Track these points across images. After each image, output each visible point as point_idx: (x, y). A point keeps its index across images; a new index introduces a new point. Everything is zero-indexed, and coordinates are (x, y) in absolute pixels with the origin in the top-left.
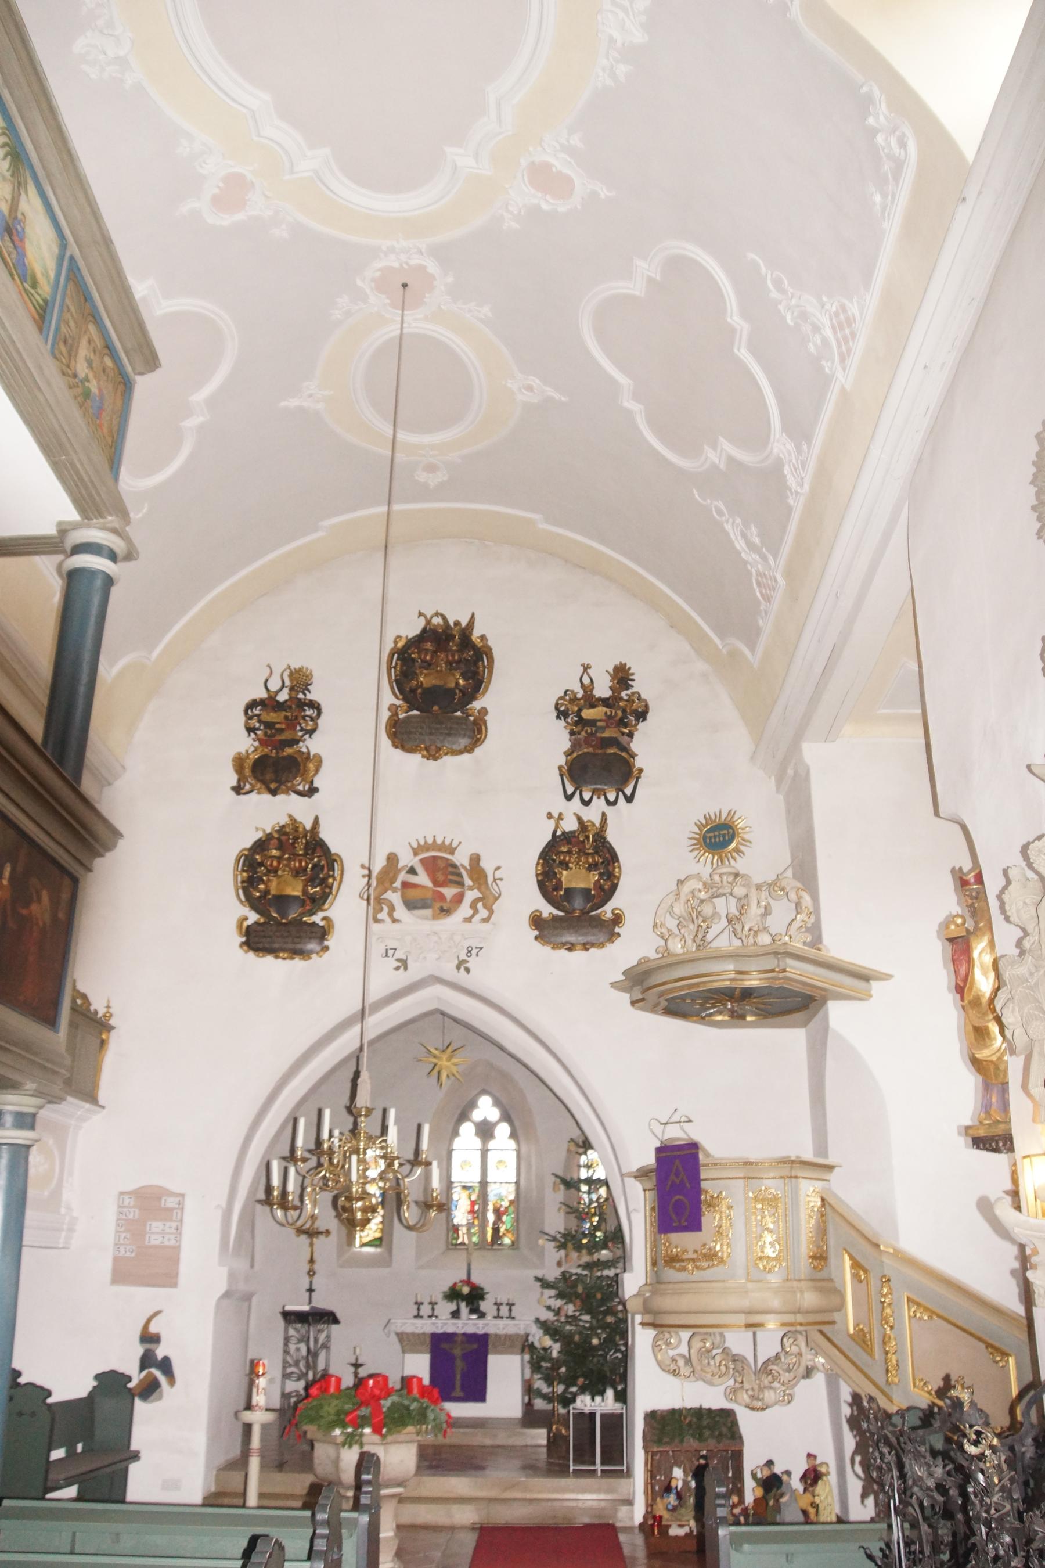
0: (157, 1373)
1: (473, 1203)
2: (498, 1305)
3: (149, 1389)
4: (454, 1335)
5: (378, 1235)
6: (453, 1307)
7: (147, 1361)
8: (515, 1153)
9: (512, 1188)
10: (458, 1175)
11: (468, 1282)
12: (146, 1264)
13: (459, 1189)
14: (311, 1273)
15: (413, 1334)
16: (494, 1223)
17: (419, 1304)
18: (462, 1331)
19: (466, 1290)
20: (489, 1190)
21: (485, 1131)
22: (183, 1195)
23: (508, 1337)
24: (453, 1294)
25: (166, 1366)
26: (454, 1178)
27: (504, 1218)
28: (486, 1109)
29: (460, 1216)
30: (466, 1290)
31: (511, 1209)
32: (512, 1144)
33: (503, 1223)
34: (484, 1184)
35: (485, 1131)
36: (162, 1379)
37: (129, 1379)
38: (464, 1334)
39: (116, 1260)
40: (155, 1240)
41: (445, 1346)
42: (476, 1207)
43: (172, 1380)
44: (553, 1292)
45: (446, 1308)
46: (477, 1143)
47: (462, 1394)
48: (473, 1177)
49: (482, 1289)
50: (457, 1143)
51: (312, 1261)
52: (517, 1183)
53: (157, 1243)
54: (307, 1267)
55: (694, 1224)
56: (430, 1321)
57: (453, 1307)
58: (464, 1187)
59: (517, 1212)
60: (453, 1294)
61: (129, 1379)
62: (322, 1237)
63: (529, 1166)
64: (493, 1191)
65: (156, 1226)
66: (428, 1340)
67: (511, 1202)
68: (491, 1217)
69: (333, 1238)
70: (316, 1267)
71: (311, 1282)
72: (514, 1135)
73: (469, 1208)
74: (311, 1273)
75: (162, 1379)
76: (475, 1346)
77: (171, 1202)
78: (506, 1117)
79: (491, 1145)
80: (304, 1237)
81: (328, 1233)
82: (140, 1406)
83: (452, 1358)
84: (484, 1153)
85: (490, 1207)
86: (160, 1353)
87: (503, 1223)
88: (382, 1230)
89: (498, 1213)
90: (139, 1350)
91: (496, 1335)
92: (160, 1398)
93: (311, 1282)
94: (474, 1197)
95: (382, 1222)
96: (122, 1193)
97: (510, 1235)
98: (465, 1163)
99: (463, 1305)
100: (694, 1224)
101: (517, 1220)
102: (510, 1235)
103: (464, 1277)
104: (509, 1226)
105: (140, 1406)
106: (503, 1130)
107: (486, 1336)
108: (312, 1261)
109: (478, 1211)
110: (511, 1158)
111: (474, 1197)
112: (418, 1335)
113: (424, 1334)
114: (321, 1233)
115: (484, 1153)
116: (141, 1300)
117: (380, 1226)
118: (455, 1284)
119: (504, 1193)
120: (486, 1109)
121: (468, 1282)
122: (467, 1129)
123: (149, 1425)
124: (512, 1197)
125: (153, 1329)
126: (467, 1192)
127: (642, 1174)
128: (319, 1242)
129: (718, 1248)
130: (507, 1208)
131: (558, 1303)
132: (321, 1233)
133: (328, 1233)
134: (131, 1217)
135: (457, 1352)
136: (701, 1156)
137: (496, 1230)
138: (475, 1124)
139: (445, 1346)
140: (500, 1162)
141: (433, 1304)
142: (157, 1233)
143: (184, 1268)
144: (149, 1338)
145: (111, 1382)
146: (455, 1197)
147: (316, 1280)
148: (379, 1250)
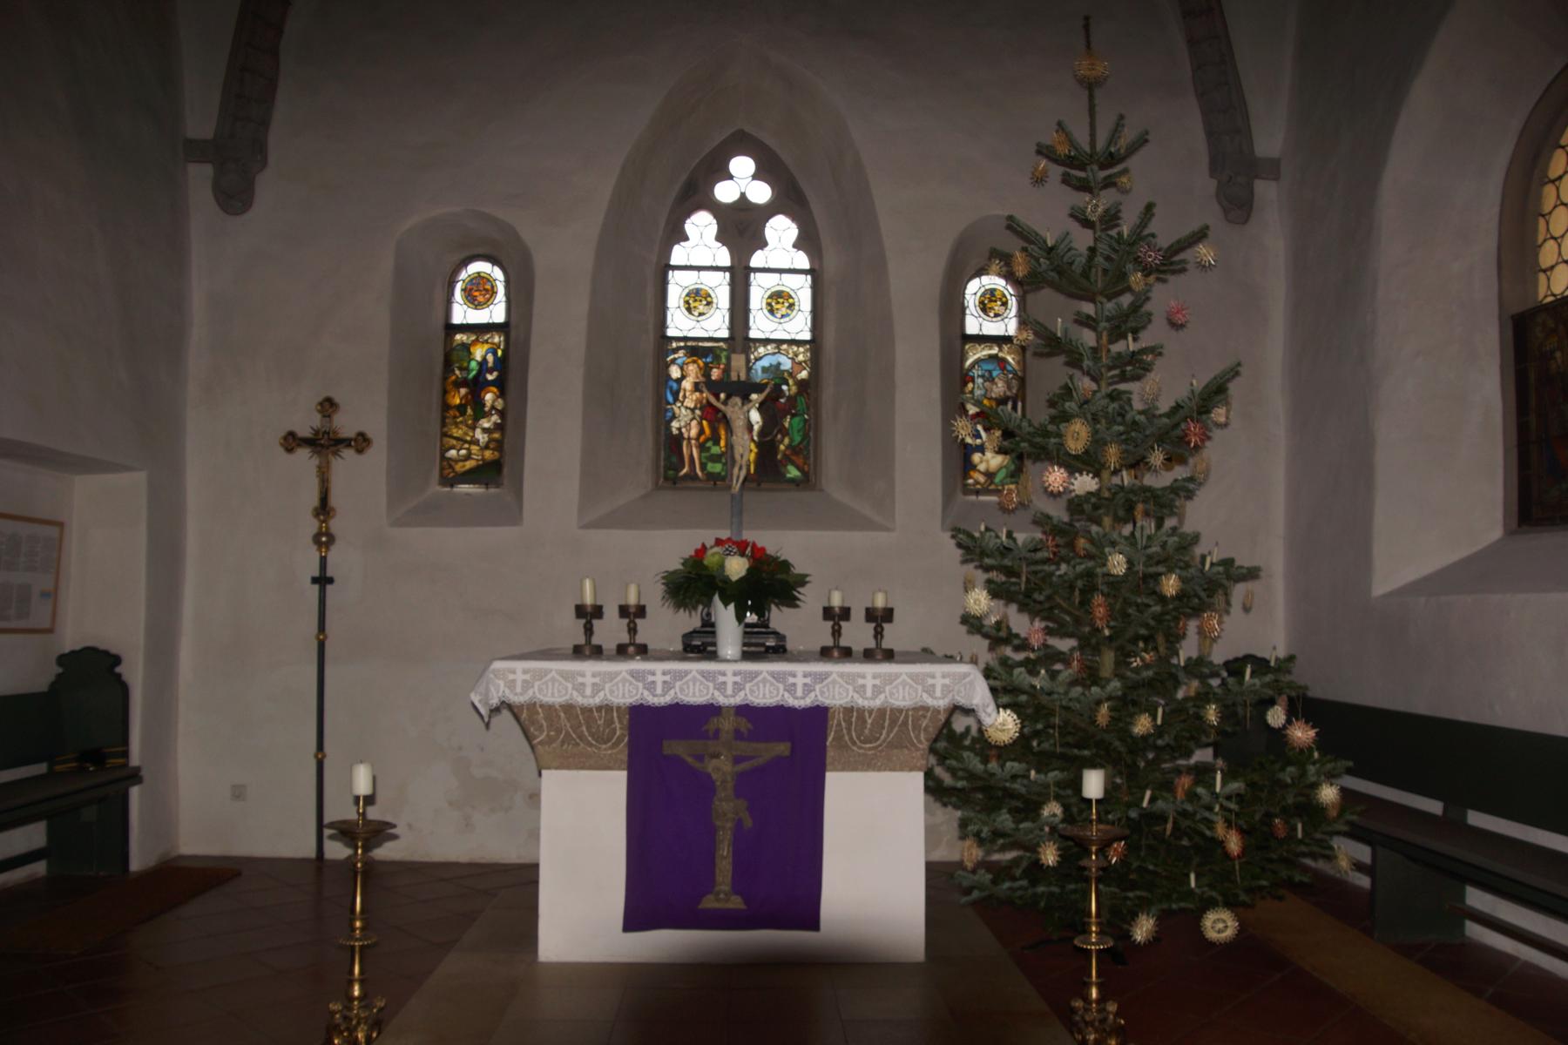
2: (836, 616)
4: (711, 710)
6: (690, 621)
14: (324, 540)
15: (569, 708)
17: (589, 614)
18: (737, 700)
19: (736, 567)
21: (742, 228)
23: (890, 717)
28: (742, 181)
30: (736, 567)
33: (785, 432)
35: (742, 228)
38: (745, 710)
41: (676, 748)
45: (668, 624)
46: (723, 257)
47: (736, 903)
49: (786, 565)
51: (324, 509)
54: (312, 526)
56: (623, 667)
57: (690, 621)
62: (348, 454)
66: (620, 728)
69: (377, 456)
70: (335, 525)
71: (323, 562)
74: (324, 540)
76: (783, 748)
78: (789, 200)
79: (757, 260)
80: (303, 453)
81: (361, 442)
83: (704, 787)
84: (740, 277)
87: (785, 432)
91: (848, 710)
93: (323, 562)
98: (697, 299)
99: (726, 617)
104: (798, 439)
106: (781, 231)
107: (818, 715)
108: (324, 509)
112: (587, 711)
113: (606, 708)
114: (347, 442)
115: (740, 277)
118: (702, 551)
119: (786, 364)
120: (742, 181)
122: (701, 225)
128: (345, 464)
132: (347, 442)
133: (361, 442)
135: (721, 768)
137: (766, 446)
139: (676, 748)
141: (633, 614)
146: (675, 372)
147: (334, 556)
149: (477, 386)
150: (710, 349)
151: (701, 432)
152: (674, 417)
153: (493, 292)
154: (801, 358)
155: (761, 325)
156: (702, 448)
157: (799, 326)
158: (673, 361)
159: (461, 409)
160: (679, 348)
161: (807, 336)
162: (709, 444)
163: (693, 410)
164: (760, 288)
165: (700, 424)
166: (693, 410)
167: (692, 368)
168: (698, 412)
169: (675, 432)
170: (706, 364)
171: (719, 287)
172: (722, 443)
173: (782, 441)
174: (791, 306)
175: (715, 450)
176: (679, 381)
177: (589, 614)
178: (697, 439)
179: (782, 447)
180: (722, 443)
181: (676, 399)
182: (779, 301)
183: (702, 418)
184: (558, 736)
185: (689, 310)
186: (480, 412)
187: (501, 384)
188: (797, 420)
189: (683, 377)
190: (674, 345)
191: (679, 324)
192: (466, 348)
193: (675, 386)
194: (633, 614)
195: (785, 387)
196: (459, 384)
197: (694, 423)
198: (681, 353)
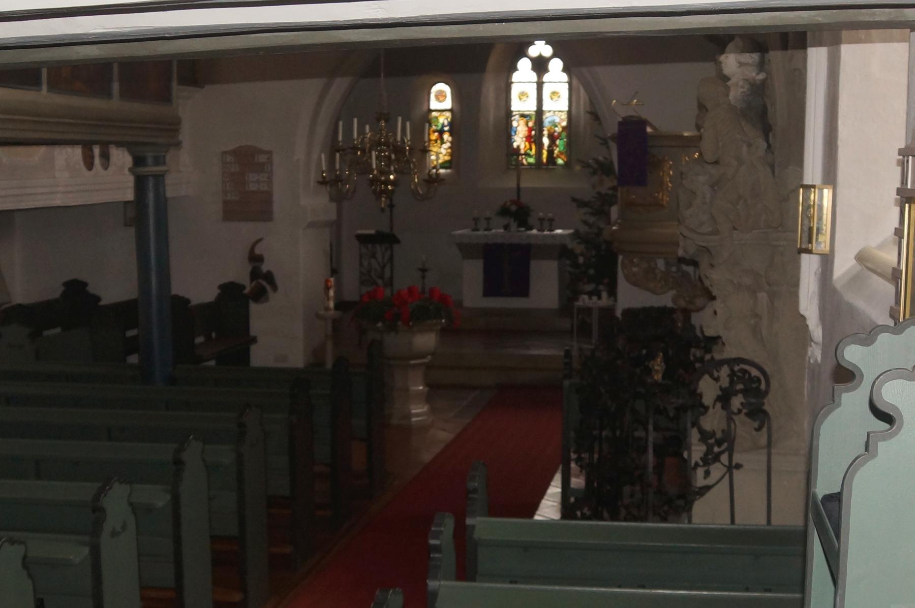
0: (264, 283)
1: (530, 130)
2: (541, 220)
3: (259, 295)
5: (447, 158)
6: (504, 221)
7: (255, 274)
8: (567, 85)
9: (564, 116)
10: (517, 105)
11: (517, 202)
12: (248, 203)
13: (517, 117)
16: (549, 146)
17: (476, 220)
19: (514, 208)
20: (544, 117)
21: (540, 65)
22: (270, 153)
24: (504, 212)
25: (269, 277)
26: (513, 109)
27: (558, 142)
29: (519, 141)
30: (514, 208)
31: (564, 134)
32: (565, 77)
34: (540, 112)
35: (540, 65)
36: (268, 288)
37: (244, 287)
39: (225, 203)
40: (253, 187)
42: (533, 133)
43: (275, 288)
44: (586, 210)
46: (534, 76)
48: (530, 106)
50: (516, 77)
52: (569, 113)
53: (255, 189)
55: (641, 181)
58: (523, 116)
59: (569, 137)
60: (504, 212)
61: (244, 287)
63: (579, 97)
64: (547, 119)
65: (252, 177)
67: (564, 128)
68: (546, 141)
72: (566, 69)
73: (526, 133)
75: (268, 288)
77: (262, 158)
79: (546, 78)
82: (254, 307)
84: (540, 85)
85: (545, 133)
86: (265, 268)
87: (557, 146)
88: (451, 155)
89: (552, 137)
90: (249, 268)
92: (267, 300)
94: (531, 124)
95: (450, 148)
96: (224, 153)
97: (563, 157)
98: (523, 95)
99: (512, 220)
100: (641, 181)
101: (569, 145)
102: (563, 157)
103: (515, 198)
104: (562, 148)
105: (254, 307)
106: (556, 65)
109: (534, 138)
110: (564, 90)
111: (531, 124)
115: (540, 85)
116: (247, 231)
117: (449, 151)
119: (557, 120)
121: (517, 202)
122: (524, 64)
123: (261, 319)
124: (564, 124)
125: (257, 251)
126: (525, 119)
127: (613, 138)
129: (660, 197)
130: (560, 134)
131: (592, 220)
134: (233, 170)
136: (649, 130)
137: (550, 152)
138: (532, 59)
140: (554, 93)
142: (254, 183)
143: (276, 207)
144: (255, 259)
145: (230, 290)
146: (515, 124)
148: (449, 171)
149: (441, 132)
153: (445, 97)
157: (563, 104)
159: (436, 141)
161: (567, 109)
164: (547, 90)
171: (532, 90)
177: (476, 220)
179: (556, 152)
184: (467, 250)
186: (443, 142)
187: (451, 132)
192: (437, 118)
194: (488, 219)
196: (434, 132)
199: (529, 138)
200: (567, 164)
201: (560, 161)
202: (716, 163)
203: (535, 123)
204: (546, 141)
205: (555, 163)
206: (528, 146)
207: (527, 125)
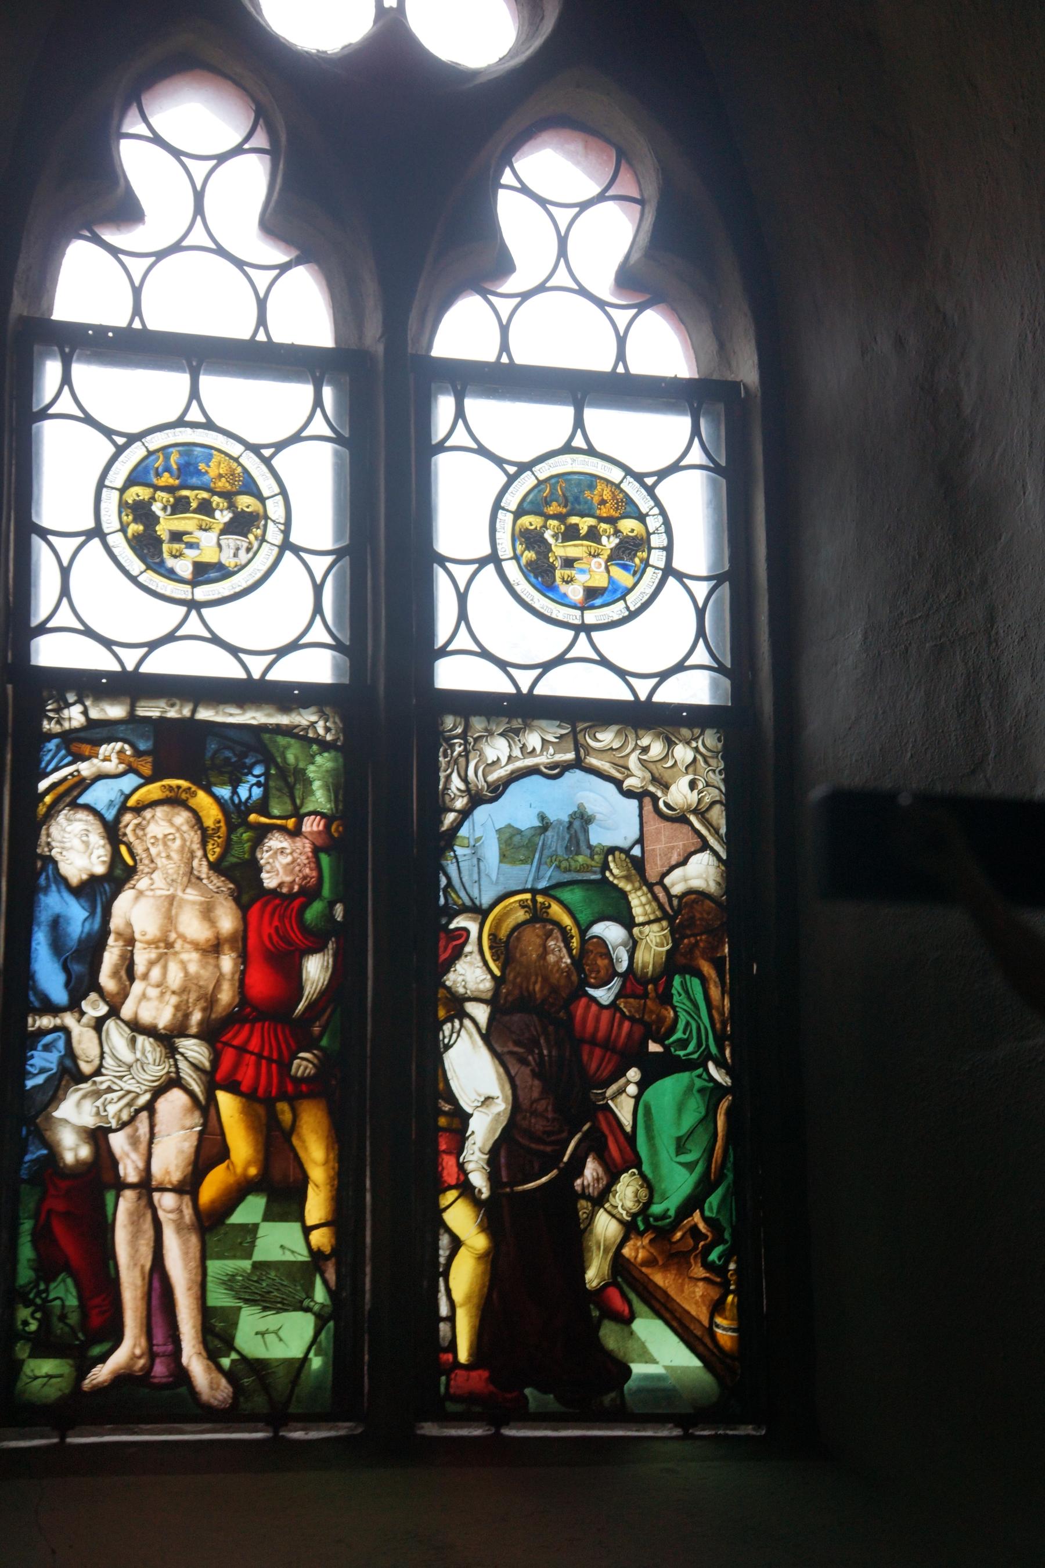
1: (271, 927)
21: (384, 175)
29: (125, 1091)
31: (696, 1005)
33: (621, 1154)
46: (304, 311)
68: (474, 1073)
79: (463, 331)
84: (385, 410)
87: (621, 1154)
89: (536, 1022)
94: (281, 861)
102: (693, 1296)
104: (678, 1183)
106: (566, 224)
109: (328, 1028)
115: (385, 410)
119: (616, 822)
122: (190, 156)
137: (535, 1226)
150: (255, 743)
151: (210, 1150)
152: (70, 1074)
154: (680, 794)
155: (489, 633)
156: (211, 1227)
157: (664, 643)
158: (72, 794)
160: (97, 733)
162: (251, 1210)
163: (167, 1040)
165: (205, 1108)
166: (167, 1040)
167: (165, 836)
168: (194, 1050)
169: (73, 1149)
170: (235, 814)
171: (293, 448)
172: (317, 1206)
173: (600, 1200)
174: (629, 550)
175: (280, 1242)
176: (100, 891)
178: (189, 1186)
179: (605, 1227)
180: (317, 1206)
181: (83, 984)
182: (568, 521)
183: (214, 1079)
185: (147, 546)
188: (669, 1089)
189: (119, 875)
190: (75, 717)
191: (95, 611)
193: (77, 917)
195: (611, 932)
197: (174, 1102)
198: (109, 756)
199: (247, 1040)
200: (745, 1380)
201: (660, 1353)
202: (262, 1334)
203: (339, 844)
204: (474, 1073)
205: (601, 1378)
206: (241, 1147)
207: (239, 873)
